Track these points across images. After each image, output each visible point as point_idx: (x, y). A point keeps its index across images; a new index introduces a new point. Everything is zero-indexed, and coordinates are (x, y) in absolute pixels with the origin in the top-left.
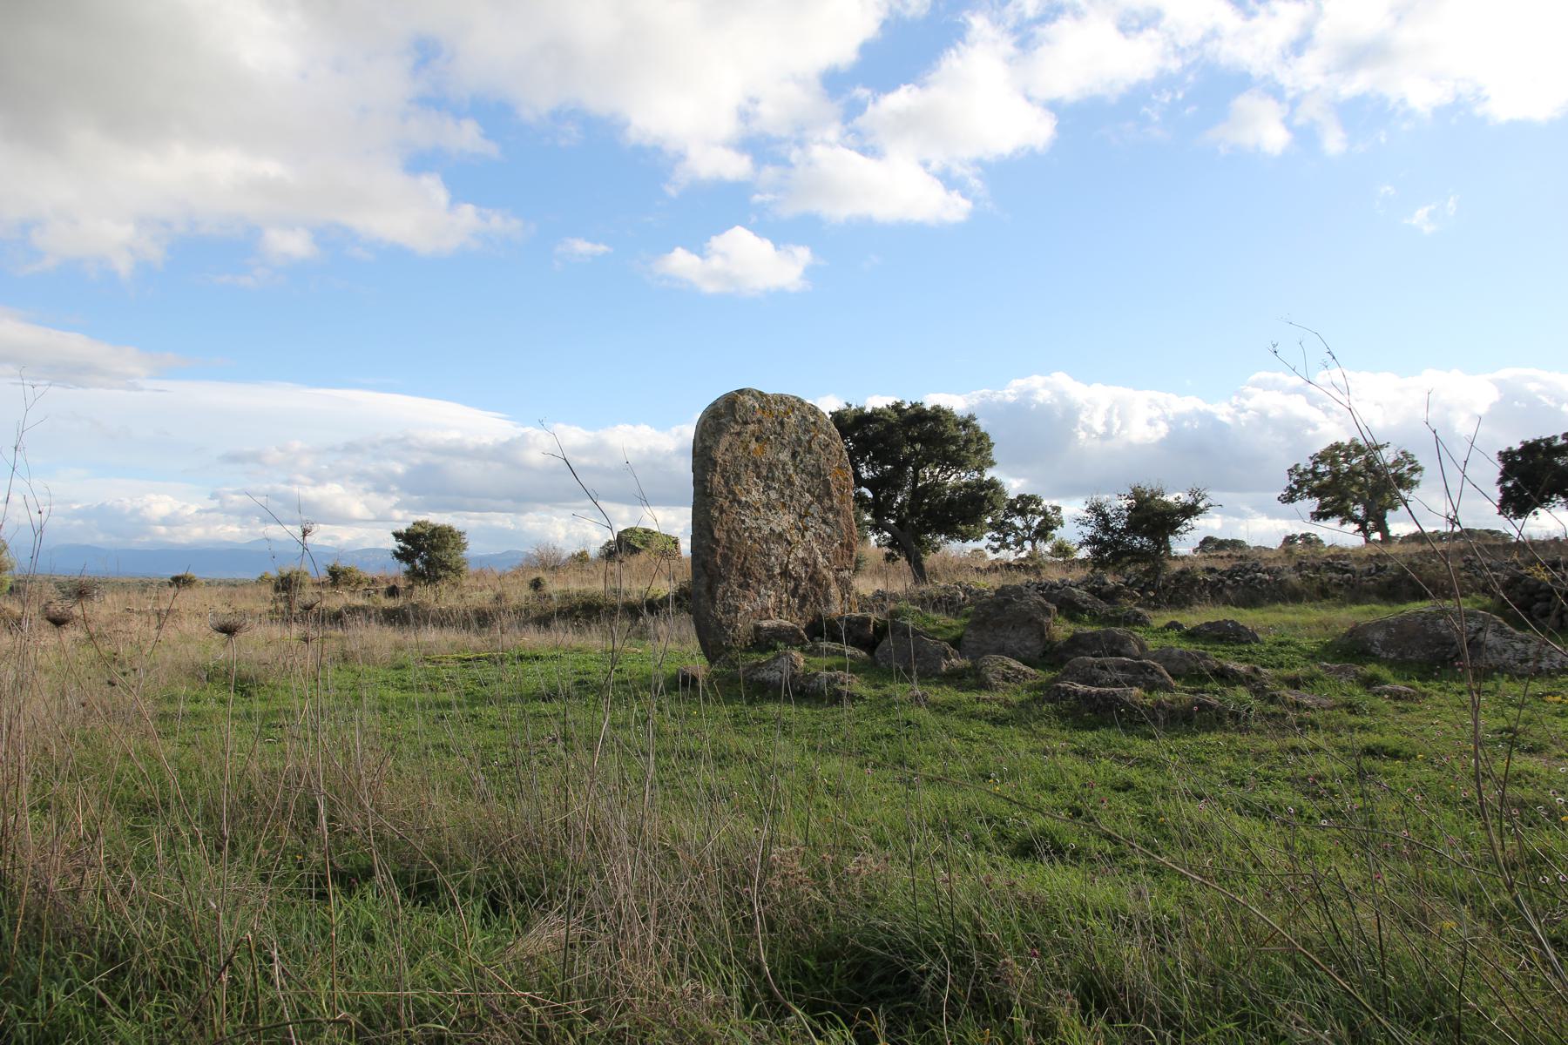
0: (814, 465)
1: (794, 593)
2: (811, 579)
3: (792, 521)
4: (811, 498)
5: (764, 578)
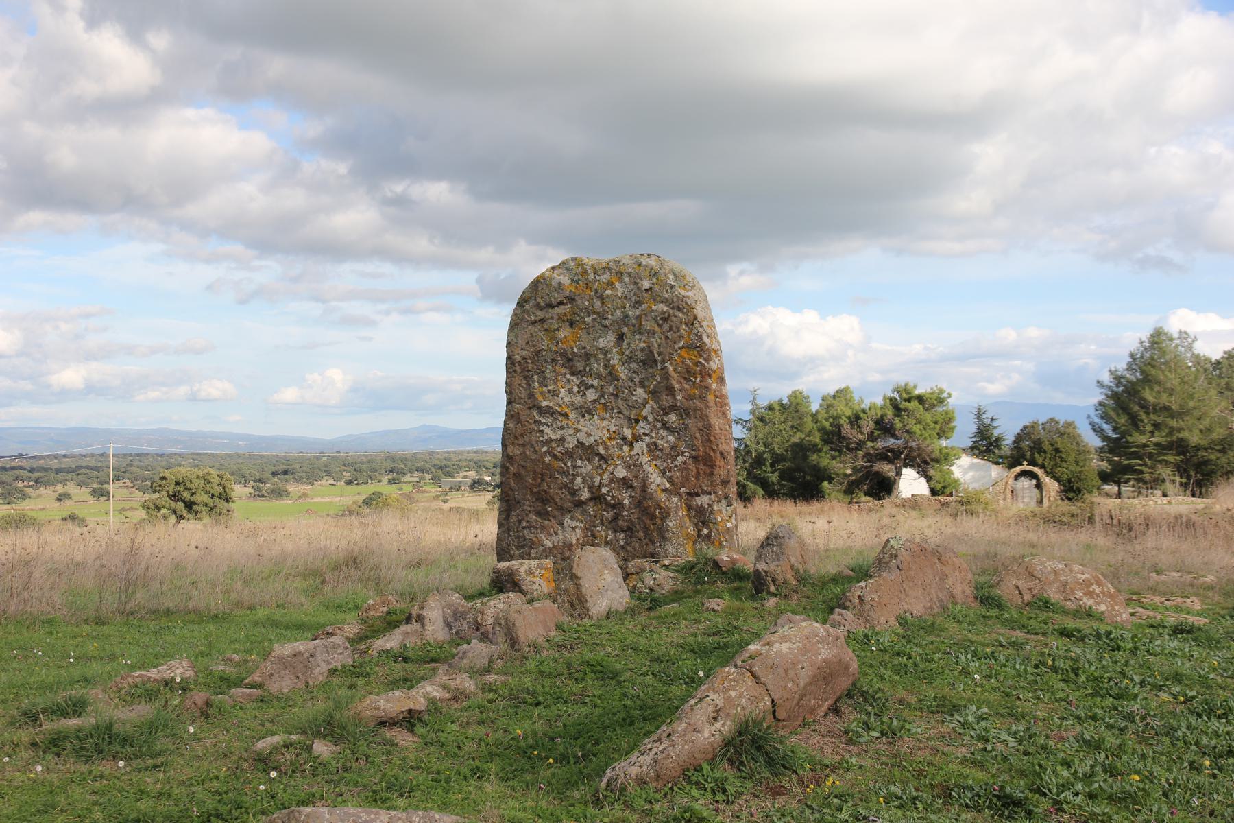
0: (642, 350)
1: (614, 524)
2: (639, 504)
3: (613, 428)
4: (645, 396)
5: (568, 505)
